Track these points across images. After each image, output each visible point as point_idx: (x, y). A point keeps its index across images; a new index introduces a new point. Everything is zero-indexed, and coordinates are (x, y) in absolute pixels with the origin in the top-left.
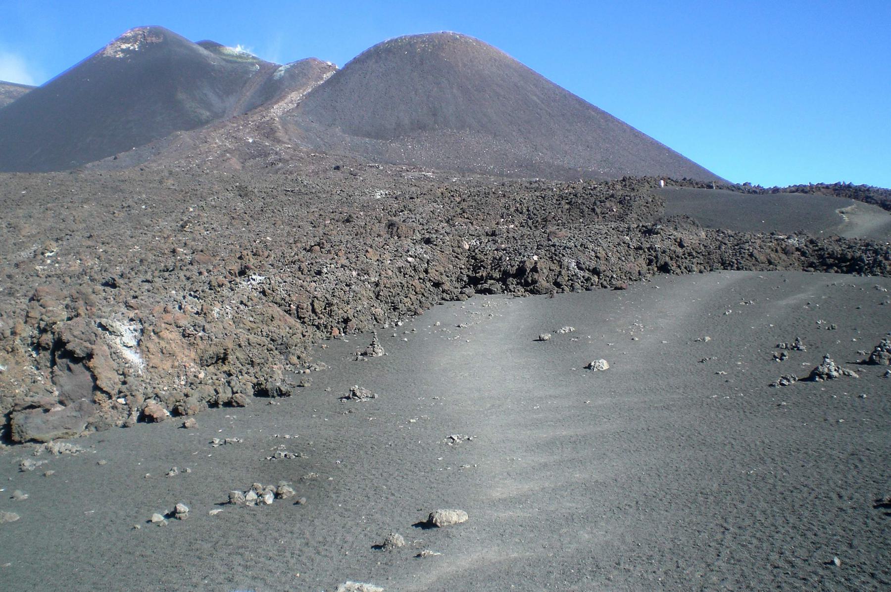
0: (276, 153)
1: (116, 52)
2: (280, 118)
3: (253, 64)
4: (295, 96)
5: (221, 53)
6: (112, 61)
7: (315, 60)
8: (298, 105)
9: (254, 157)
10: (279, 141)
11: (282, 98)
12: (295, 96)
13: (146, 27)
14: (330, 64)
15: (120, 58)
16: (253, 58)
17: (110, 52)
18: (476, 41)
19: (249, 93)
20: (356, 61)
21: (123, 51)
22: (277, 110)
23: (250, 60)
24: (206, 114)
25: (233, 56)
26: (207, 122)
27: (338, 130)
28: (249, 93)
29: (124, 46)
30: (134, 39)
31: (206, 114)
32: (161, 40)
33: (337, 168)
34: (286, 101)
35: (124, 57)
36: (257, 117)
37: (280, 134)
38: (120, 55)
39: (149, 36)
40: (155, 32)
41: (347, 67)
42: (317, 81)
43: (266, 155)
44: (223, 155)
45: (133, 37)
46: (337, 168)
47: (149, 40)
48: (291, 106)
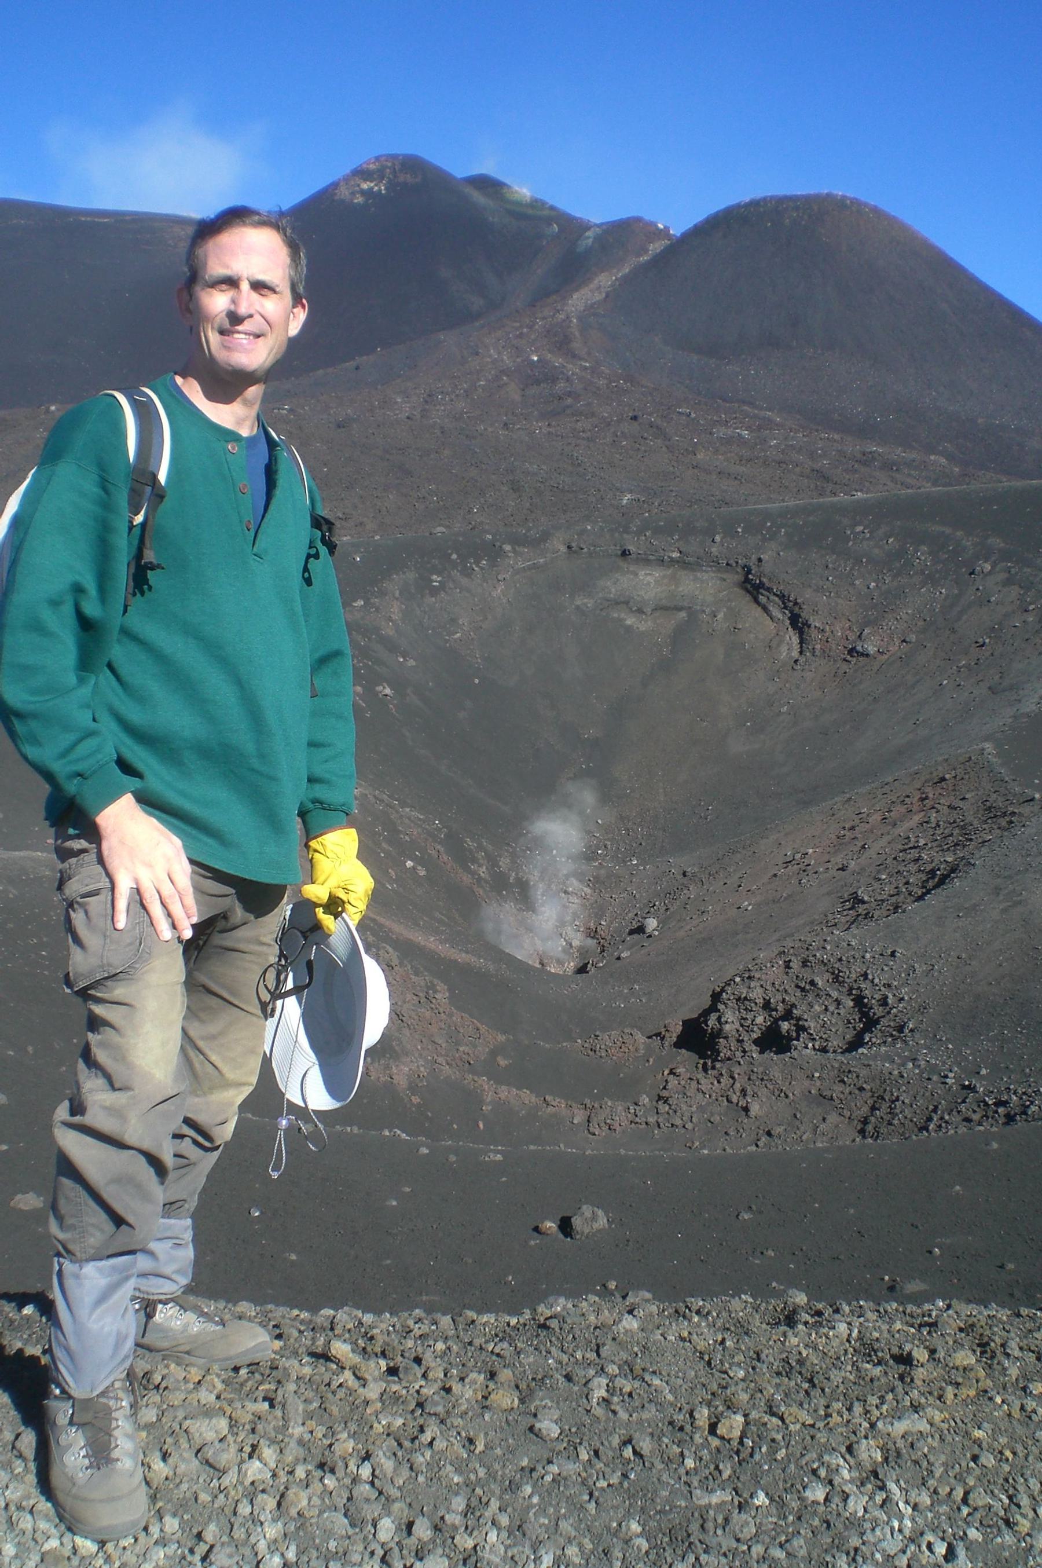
0: (568, 380)
1: (353, 194)
2: (580, 319)
3: (549, 221)
4: (605, 280)
7: (638, 220)
8: (607, 296)
9: (538, 382)
10: (574, 356)
12: (605, 280)
13: (394, 157)
14: (661, 226)
15: (359, 204)
16: (552, 208)
17: (344, 193)
18: (875, 210)
21: (363, 192)
22: (579, 300)
23: (546, 213)
24: (477, 303)
25: (519, 204)
29: (365, 186)
31: (477, 303)
32: (419, 180)
33: (635, 418)
34: (592, 286)
36: (547, 312)
37: (577, 345)
38: (359, 200)
40: (412, 164)
41: (686, 237)
42: (639, 255)
43: (554, 380)
44: (497, 378)
45: (379, 170)
46: (635, 418)
47: (401, 178)
48: (598, 297)
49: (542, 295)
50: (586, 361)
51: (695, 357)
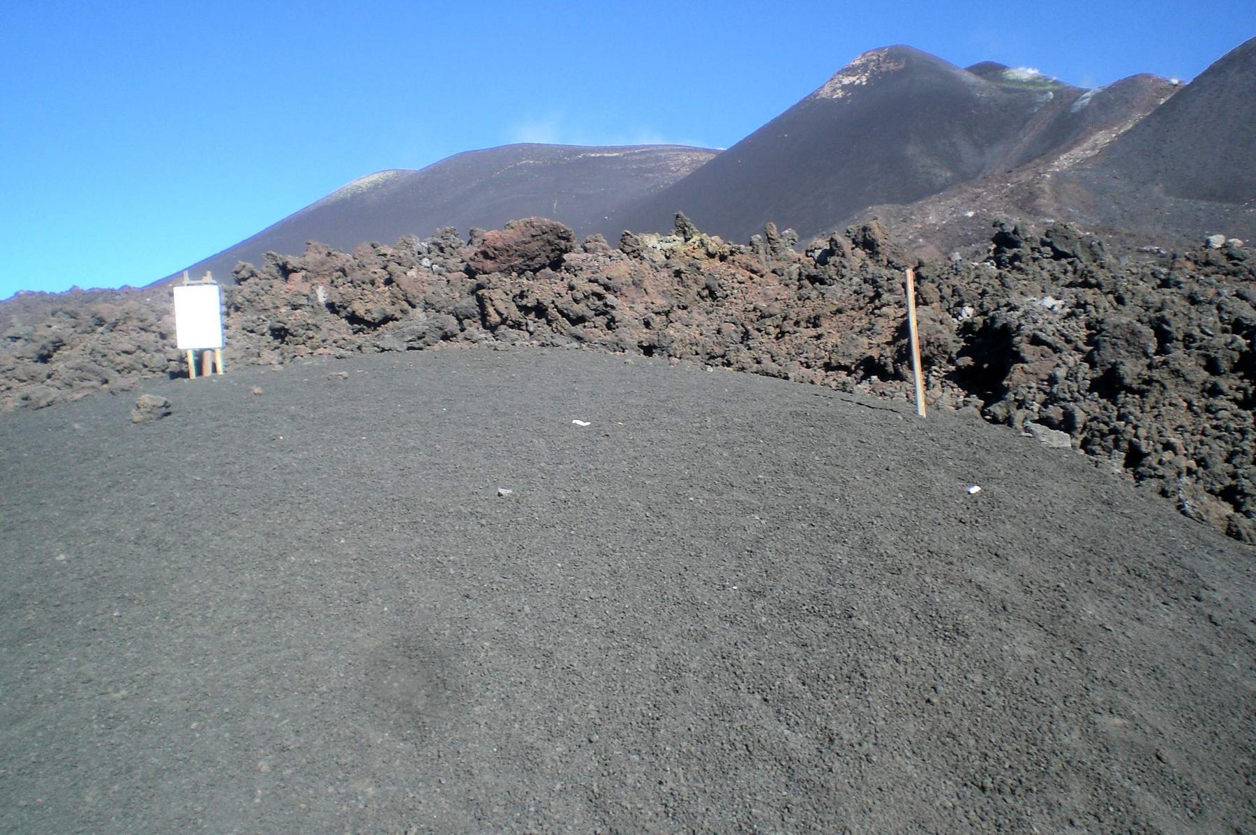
4: (1103, 138)
5: (1003, 80)
6: (828, 104)
7: (1148, 76)
11: (1077, 143)
12: (1103, 138)
13: (881, 50)
14: (1175, 81)
19: (1027, 139)
20: (1214, 71)
21: (844, 88)
26: (944, 187)
27: (1157, 190)
28: (1027, 139)
29: (846, 81)
30: (864, 67)
32: (901, 66)
34: (1085, 145)
35: (845, 98)
37: (1044, 202)
38: (840, 94)
39: (884, 61)
40: (896, 54)
41: (1197, 81)
45: (863, 65)
49: (1026, 159)
50: (1052, 217)
51: (1203, 204)
